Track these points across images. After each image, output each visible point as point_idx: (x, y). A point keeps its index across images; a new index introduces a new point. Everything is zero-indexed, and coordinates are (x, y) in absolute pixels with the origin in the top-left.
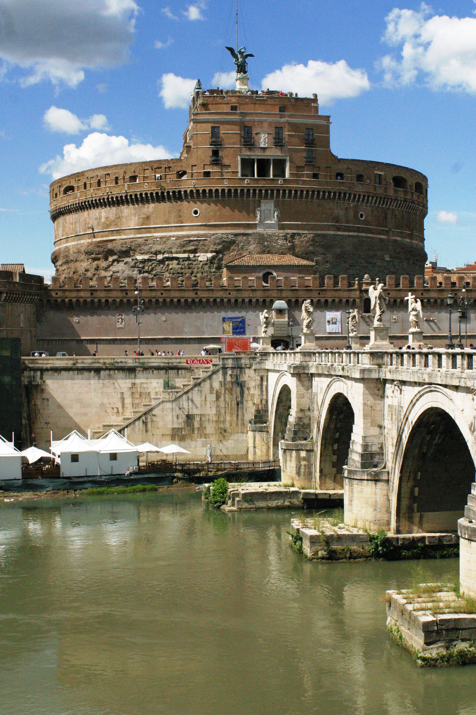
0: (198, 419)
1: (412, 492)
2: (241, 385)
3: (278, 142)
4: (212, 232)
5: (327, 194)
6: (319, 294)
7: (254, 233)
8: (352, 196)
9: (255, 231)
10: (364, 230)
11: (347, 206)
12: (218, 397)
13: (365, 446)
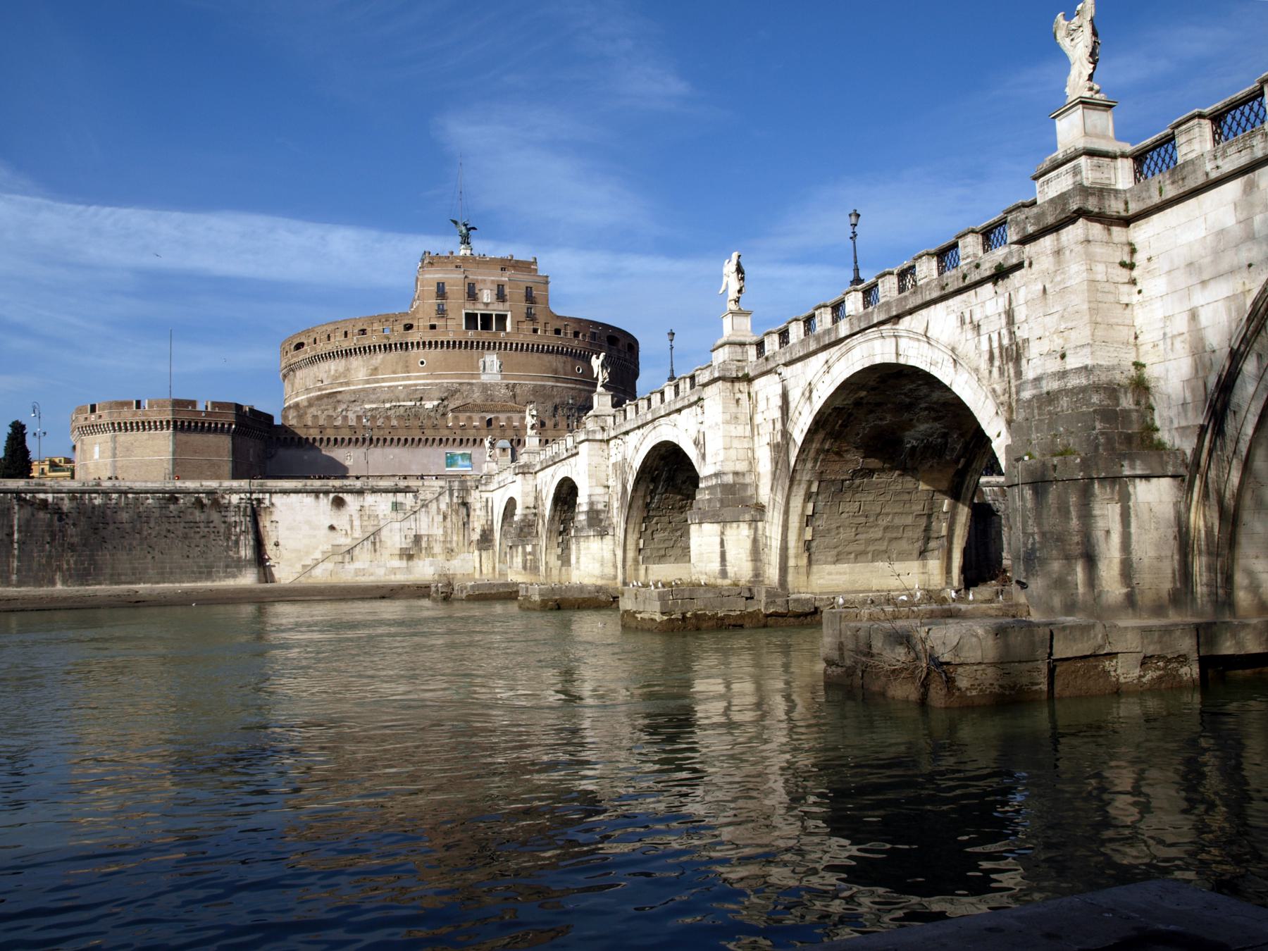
0: (425, 539)
1: (638, 544)
2: (465, 504)
3: (501, 296)
12: (445, 518)
13: (591, 504)
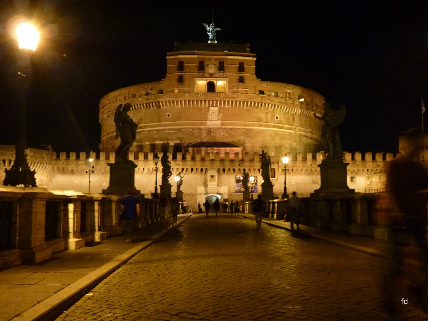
4: (177, 127)
5: (253, 103)
6: (239, 165)
7: (205, 128)
8: (270, 105)
9: (205, 127)
10: (278, 127)
11: (267, 111)
